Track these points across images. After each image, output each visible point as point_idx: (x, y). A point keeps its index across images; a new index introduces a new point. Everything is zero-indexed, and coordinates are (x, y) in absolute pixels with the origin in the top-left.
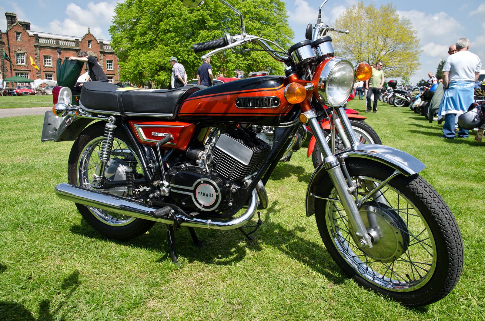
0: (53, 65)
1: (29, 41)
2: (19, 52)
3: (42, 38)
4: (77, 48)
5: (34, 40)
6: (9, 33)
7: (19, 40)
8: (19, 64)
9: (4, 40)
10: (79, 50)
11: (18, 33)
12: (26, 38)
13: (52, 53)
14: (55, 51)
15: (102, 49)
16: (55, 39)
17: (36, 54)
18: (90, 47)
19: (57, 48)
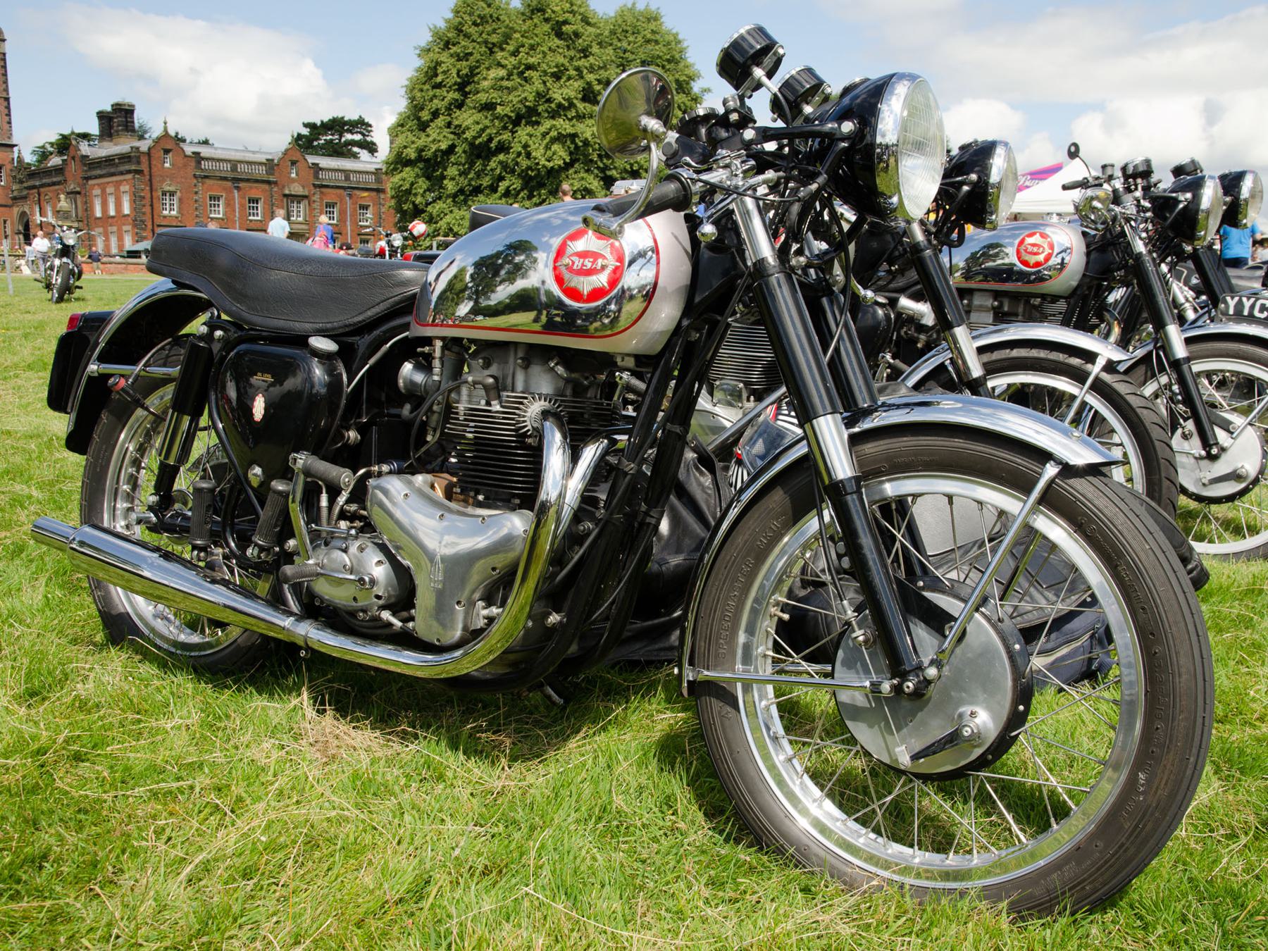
1: (185, 166)
2: (167, 188)
3: (207, 159)
4: (272, 179)
5: (193, 164)
6: (153, 151)
7: (167, 165)
8: (166, 213)
9: (144, 166)
10: (275, 183)
11: (167, 151)
12: (180, 161)
13: (225, 189)
14: (229, 184)
15: (317, 178)
16: (230, 161)
19: (235, 180)
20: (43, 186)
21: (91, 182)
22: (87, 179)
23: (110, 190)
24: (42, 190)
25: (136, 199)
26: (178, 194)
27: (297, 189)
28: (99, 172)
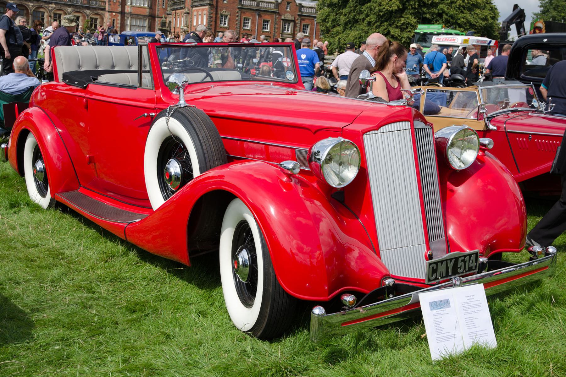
0: (251, 27)
17: (237, 16)
18: (288, 10)
20: (177, 9)
21: (194, 9)
22: (192, 7)
23: (200, 13)
24: (177, 11)
25: (210, 18)
26: (228, 17)
27: (289, 16)
28: (197, 4)
